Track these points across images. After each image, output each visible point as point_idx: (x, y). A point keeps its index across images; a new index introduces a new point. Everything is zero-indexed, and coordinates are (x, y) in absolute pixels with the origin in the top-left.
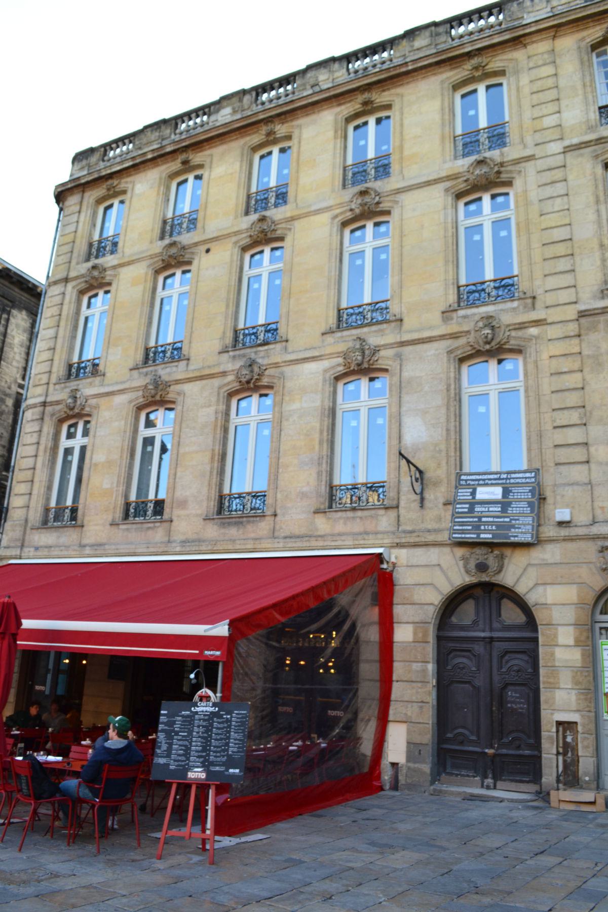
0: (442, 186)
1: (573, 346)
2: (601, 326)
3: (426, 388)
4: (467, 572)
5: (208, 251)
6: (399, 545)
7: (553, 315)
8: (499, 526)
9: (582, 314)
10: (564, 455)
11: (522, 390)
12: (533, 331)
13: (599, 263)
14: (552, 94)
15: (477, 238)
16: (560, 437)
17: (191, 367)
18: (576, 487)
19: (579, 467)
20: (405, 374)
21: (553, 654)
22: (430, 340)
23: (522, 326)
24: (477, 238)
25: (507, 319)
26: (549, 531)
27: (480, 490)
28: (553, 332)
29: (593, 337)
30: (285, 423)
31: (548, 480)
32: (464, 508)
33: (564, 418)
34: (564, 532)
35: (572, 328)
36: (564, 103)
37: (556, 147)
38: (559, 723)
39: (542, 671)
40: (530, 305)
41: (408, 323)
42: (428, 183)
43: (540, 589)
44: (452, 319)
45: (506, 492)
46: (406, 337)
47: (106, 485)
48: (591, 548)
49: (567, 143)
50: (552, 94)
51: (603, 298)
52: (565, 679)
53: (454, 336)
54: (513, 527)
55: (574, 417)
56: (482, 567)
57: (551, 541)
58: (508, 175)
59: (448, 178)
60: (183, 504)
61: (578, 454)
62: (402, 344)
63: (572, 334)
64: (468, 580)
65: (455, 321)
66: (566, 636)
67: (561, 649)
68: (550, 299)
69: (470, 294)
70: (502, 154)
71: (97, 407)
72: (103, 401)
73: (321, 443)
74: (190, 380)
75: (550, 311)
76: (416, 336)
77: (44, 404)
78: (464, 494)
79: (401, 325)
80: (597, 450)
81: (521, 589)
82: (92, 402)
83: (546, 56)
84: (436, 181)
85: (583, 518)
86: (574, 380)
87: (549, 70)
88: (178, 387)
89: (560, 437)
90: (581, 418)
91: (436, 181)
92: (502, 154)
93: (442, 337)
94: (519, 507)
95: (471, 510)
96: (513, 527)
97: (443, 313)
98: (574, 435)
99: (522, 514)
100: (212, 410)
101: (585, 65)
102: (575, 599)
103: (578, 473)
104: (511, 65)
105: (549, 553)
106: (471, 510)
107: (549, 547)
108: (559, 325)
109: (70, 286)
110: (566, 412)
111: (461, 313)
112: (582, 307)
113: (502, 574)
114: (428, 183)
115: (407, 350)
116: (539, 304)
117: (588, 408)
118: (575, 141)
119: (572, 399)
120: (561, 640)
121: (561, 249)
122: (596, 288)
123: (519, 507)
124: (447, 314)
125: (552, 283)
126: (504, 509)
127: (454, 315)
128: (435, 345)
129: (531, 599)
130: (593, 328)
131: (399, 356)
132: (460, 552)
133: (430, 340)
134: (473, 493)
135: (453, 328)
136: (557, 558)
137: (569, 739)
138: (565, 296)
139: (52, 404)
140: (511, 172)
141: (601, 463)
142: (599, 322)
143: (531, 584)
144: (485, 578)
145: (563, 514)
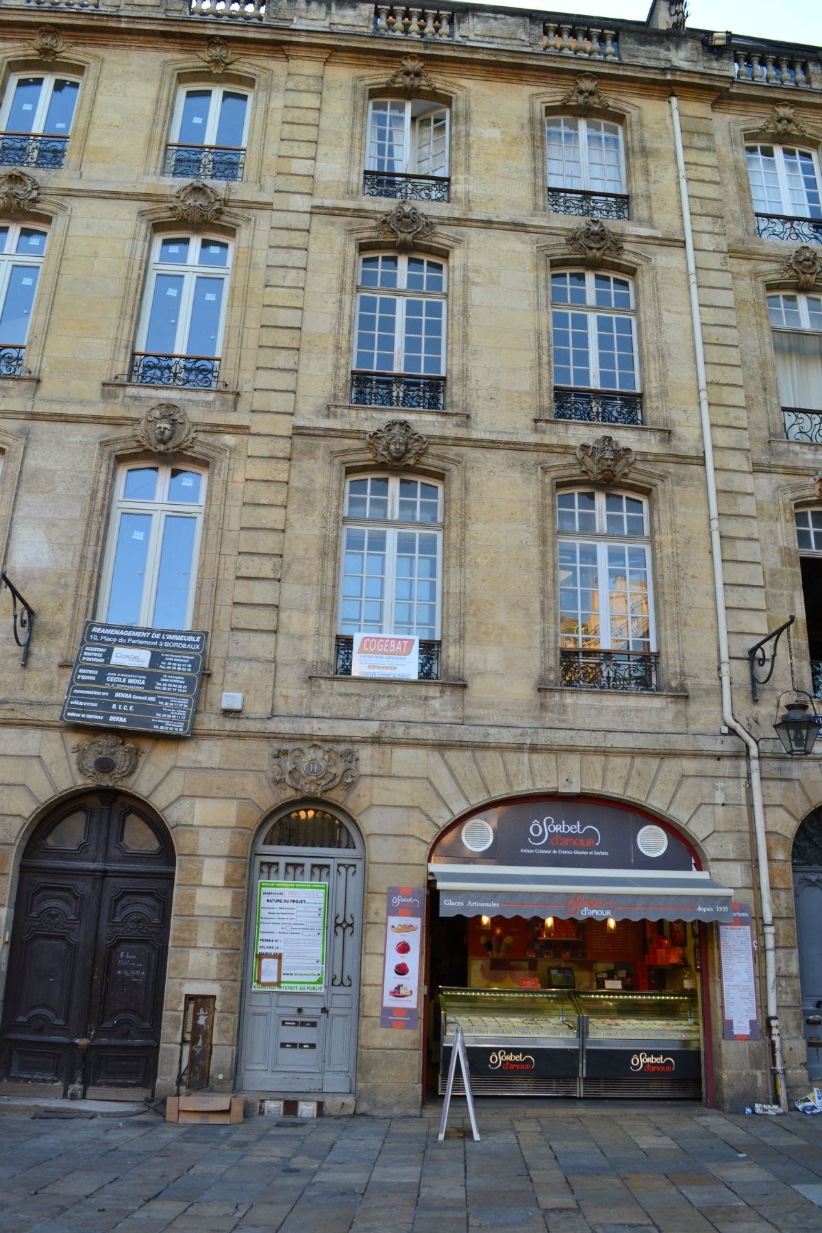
0: (136, 206)
1: (279, 471)
2: (320, 453)
3: (60, 490)
4: (81, 770)
7: (260, 424)
8: (140, 707)
9: (298, 431)
10: (244, 617)
11: (200, 519)
12: (229, 440)
13: (330, 369)
14: (311, 133)
15: (172, 292)
16: (242, 592)
18: (254, 664)
19: (264, 637)
20: (31, 462)
21: (192, 898)
23: (215, 429)
24: (172, 292)
25: (196, 415)
26: (210, 722)
27: (117, 650)
28: (256, 446)
29: (307, 464)
31: (218, 649)
32: (90, 675)
33: (252, 567)
34: (230, 725)
35: (282, 447)
36: (322, 150)
37: (303, 203)
38: (189, 998)
39: (174, 922)
40: (231, 403)
41: (46, 389)
42: (116, 196)
43: (186, 803)
44: (116, 397)
45: (156, 659)
46: (41, 408)
48: (262, 753)
49: (317, 202)
50: (311, 133)
51: (328, 416)
52: (206, 935)
53: (115, 422)
54: (160, 710)
55: (266, 568)
56: (105, 766)
57: (210, 735)
58: (232, 220)
59: (147, 197)
61: (264, 619)
62: (34, 416)
63: (281, 455)
64: (81, 782)
65: (120, 400)
66: (214, 872)
67: (204, 892)
68: (259, 401)
69: (149, 368)
70: (229, 189)
76: (57, 409)
78: (94, 655)
79: (36, 389)
80: (289, 618)
81: (158, 802)
83: (311, 81)
85: (259, 708)
86: (273, 517)
87: (311, 100)
89: (242, 592)
90: (274, 571)
92: (229, 189)
93: (96, 420)
94: (172, 683)
95: (101, 679)
96: (160, 710)
97: (104, 384)
98: (263, 593)
99: (177, 694)
101: (357, 112)
102: (233, 821)
103: (260, 645)
104: (264, 76)
105: (206, 753)
106: (101, 679)
107: (206, 744)
108: (266, 439)
110: (255, 558)
111: (131, 391)
112: (300, 423)
113: (134, 777)
114: (116, 196)
115: (40, 427)
116: (243, 405)
117: (286, 559)
118: (328, 203)
119: (268, 543)
120: (207, 878)
121: (284, 338)
122: (321, 401)
123: (172, 683)
124: (110, 387)
125: (265, 379)
126: (150, 684)
127: (121, 392)
128: (85, 428)
129: (172, 817)
130: (310, 453)
131: (25, 434)
132: (74, 739)
134: (108, 655)
135: (115, 409)
136: (216, 761)
137: (201, 1021)
138: (280, 402)
140: (236, 216)
141: (293, 636)
142: (318, 447)
143: (173, 796)
144: (107, 781)
145: (231, 700)
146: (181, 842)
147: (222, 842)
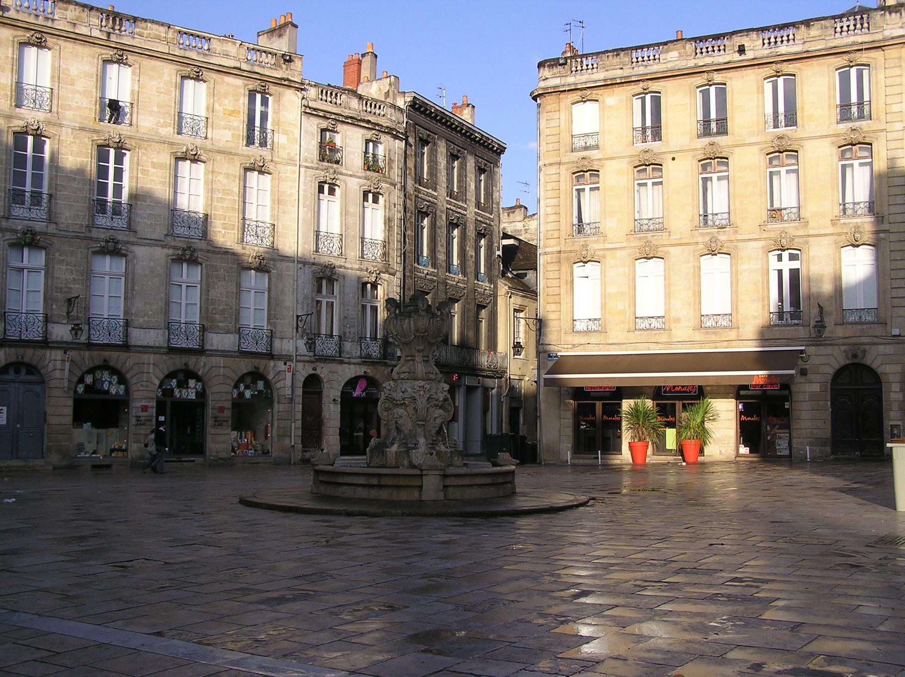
0: (829, 139)
4: (848, 358)
5: (673, 159)
6: (810, 345)
17: (672, 237)
22: (825, 235)
28: (893, 237)
30: (740, 277)
41: (811, 224)
42: (822, 137)
47: (620, 307)
52: (895, 406)
53: (839, 234)
60: (677, 320)
62: (809, 236)
64: (847, 362)
68: (892, 218)
71: (604, 257)
72: (608, 253)
73: (763, 289)
74: (673, 245)
75: (892, 225)
76: (817, 232)
77: (560, 252)
81: (874, 366)
82: (601, 253)
84: (826, 136)
88: (665, 249)
91: (826, 136)
100: (691, 265)
102: (900, 371)
104: (874, 62)
109: (563, 169)
114: (822, 137)
115: (811, 239)
116: (885, 220)
120: (893, 389)
124: (834, 222)
125: (893, 209)
128: (827, 237)
133: (825, 235)
139: (565, 252)
146: (883, 379)
147: (897, 378)
